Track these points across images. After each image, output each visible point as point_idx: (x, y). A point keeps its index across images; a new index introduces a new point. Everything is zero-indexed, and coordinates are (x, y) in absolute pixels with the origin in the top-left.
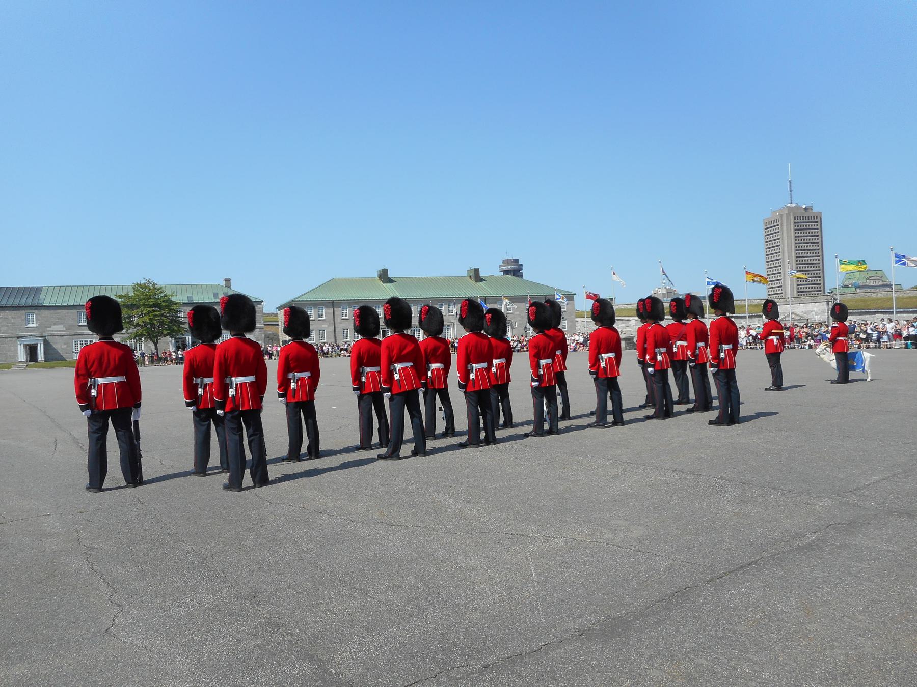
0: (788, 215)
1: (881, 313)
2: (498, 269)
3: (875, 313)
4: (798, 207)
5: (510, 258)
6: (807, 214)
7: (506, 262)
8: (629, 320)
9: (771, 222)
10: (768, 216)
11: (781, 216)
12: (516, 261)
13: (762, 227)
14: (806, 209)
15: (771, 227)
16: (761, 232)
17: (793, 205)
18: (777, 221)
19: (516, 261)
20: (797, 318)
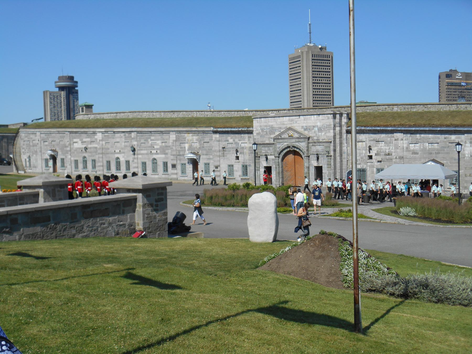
0: (307, 52)
1: (401, 131)
2: (53, 85)
3: (392, 132)
4: (315, 46)
5: (65, 74)
6: (322, 53)
7: (61, 78)
8: (94, 133)
9: (294, 58)
10: (293, 53)
11: (302, 53)
12: (71, 78)
13: (288, 62)
14: (321, 49)
15: (295, 61)
16: (287, 66)
17: (312, 45)
18: (299, 57)
19: (71, 78)
20: (296, 135)
